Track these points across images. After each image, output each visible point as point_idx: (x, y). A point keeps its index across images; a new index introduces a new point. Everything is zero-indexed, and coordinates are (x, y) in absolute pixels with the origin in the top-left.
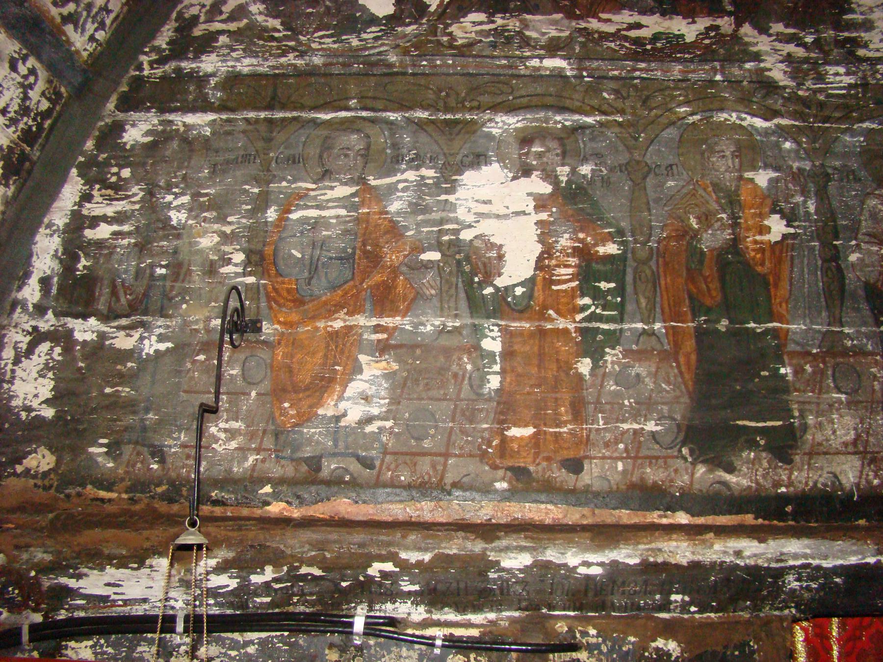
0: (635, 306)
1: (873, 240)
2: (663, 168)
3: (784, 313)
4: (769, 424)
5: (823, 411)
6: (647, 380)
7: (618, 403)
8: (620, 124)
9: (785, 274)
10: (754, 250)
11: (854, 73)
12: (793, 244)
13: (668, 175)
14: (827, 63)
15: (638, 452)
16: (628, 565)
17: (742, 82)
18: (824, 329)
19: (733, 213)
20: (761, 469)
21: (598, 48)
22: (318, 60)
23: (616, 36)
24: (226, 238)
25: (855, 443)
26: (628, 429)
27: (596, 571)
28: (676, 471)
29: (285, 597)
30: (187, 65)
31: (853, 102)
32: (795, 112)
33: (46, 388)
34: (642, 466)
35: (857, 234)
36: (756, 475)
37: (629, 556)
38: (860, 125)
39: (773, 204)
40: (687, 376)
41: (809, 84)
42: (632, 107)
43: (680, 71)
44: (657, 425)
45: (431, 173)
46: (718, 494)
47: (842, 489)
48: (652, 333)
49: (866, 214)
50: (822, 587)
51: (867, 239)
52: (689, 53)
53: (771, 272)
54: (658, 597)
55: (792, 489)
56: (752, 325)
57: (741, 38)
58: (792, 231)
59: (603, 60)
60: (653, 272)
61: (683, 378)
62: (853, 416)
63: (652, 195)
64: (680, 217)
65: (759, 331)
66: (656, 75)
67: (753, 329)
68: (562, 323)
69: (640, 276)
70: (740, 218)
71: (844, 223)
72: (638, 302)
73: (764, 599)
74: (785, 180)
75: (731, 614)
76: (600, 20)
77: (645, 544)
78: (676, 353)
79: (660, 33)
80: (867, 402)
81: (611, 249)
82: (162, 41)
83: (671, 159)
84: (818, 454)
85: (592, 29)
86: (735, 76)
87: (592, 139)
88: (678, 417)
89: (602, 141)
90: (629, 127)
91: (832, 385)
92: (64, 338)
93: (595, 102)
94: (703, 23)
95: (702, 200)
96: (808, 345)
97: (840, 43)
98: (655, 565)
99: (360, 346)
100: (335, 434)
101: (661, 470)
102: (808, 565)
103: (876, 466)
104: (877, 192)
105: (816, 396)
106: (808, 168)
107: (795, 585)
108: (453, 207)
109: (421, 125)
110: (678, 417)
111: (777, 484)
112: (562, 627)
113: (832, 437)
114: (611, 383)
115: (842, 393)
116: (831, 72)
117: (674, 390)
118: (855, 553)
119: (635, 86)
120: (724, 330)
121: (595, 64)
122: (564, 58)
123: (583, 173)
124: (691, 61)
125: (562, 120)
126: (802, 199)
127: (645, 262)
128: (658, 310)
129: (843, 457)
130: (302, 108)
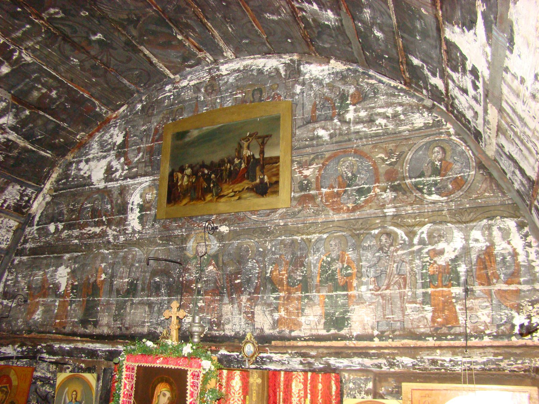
27: (68, 348)
45: (54, 268)
82: (22, 241)
97: (123, 230)
108: (56, 275)
112: (67, 360)
125: (75, 254)
130: (39, 255)
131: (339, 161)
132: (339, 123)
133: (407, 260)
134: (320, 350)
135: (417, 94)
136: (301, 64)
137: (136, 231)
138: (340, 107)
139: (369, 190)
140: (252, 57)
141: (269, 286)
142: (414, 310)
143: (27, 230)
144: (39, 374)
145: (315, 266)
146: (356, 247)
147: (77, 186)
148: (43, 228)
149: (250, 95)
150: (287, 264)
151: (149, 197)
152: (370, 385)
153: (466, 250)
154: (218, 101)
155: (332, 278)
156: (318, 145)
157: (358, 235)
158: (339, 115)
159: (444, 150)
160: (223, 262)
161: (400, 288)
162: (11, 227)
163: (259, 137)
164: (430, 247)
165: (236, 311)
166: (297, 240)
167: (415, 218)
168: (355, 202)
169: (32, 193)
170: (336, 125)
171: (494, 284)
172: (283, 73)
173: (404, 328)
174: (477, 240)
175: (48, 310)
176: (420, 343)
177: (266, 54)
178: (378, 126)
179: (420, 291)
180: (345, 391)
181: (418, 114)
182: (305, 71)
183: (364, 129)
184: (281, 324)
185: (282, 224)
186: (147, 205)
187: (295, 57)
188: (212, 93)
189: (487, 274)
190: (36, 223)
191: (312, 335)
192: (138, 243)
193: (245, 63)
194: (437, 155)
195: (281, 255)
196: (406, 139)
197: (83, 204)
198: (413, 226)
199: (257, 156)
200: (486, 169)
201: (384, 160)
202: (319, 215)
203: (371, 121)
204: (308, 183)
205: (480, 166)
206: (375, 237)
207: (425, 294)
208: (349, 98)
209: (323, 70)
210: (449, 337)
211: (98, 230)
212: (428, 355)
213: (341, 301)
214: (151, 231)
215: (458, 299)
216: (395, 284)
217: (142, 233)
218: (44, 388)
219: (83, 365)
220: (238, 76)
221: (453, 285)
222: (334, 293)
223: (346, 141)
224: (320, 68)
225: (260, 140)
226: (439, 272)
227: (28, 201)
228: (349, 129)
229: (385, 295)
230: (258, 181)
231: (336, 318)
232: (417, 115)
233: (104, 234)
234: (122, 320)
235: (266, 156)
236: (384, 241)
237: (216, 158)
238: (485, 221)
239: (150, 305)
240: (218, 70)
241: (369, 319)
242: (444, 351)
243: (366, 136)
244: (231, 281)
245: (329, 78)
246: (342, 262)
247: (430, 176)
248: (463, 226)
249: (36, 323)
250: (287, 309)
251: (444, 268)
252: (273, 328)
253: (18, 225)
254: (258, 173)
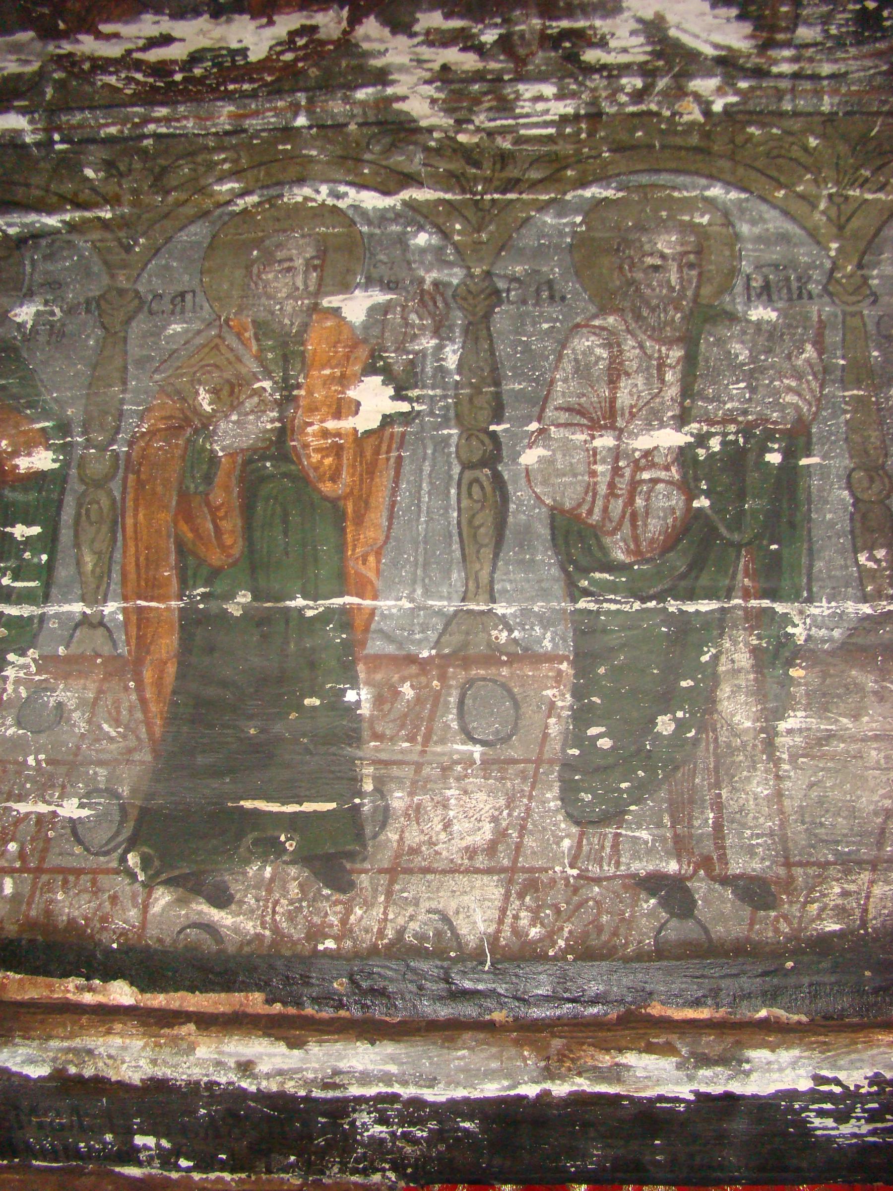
0: (72, 570)
1: (578, 419)
2: (167, 299)
3: (371, 575)
4: (308, 807)
5: (428, 780)
6: (76, 715)
7: (16, 762)
8: (105, 224)
9: (381, 499)
10: (317, 450)
11: (573, 95)
12: (403, 434)
13: (173, 313)
14: (520, 78)
15: (42, 859)
16: (27, 1077)
17: (346, 125)
18: (450, 607)
19: (285, 379)
20: (284, 902)
21: (88, 89)
23: (126, 62)
25: (491, 849)
26: (28, 814)
28: (114, 899)
31: (570, 149)
32: (451, 174)
34: (49, 888)
35: (543, 410)
36: (274, 912)
37: (31, 1061)
38: (580, 192)
39: (372, 356)
40: (153, 708)
41: (481, 119)
42: (135, 192)
43: (231, 116)
44: (81, 806)
46: (192, 948)
47: (460, 947)
48: (97, 623)
49: (568, 366)
50: (437, 1137)
51: (564, 417)
52: (252, 81)
53: (351, 493)
54: (109, 1137)
55: (349, 944)
56: (300, 602)
57: (357, 46)
58: (404, 407)
59: (92, 108)
60: (114, 502)
61: (145, 710)
62: (491, 792)
63: (134, 350)
64: (178, 392)
65: (310, 613)
66: (185, 127)
67: (300, 610)
69: (88, 510)
70: (298, 386)
71: (517, 387)
72: (79, 563)
73: (322, 1153)
74: (404, 307)
75: (264, 1176)
76: (99, 36)
77: (62, 1039)
78: (139, 662)
79: (204, 50)
80: (527, 761)
83: (185, 281)
84: (409, 871)
85: (83, 54)
86: (333, 117)
87: (48, 257)
88: (124, 791)
89: (65, 259)
90: (120, 228)
91: (455, 725)
93: (69, 187)
95: (230, 356)
96: (413, 642)
97: (551, 41)
98: (79, 1080)
101: (86, 896)
102: (394, 1098)
103: (537, 899)
104: (596, 323)
105: (419, 748)
106: (455, 281)
107: (378, 1130)
110: (124, 791)
111: (316, 933)
113: (443, 836)
114: (9, 721)
115: (475, 741)
116: (527, 95)
117: (124, 736)
118: (490, 1075)
119: (145, 151)
120: (237, 613)
121: (77, 118)
122: (23, 111)
123: (19, 320)
124: (254, 95)
126: (434, 342)
127: (99, 484)
128: (116, 576)
129: (463, 880)
137: (693, 56)
217: (759, 73)
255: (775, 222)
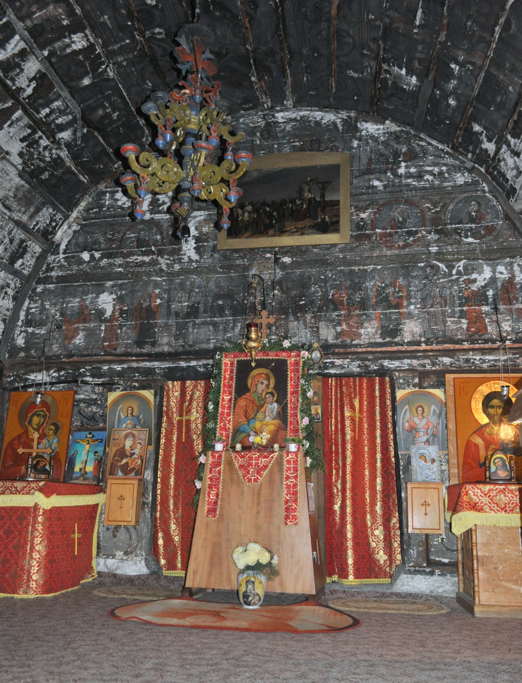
22: (74, 272)
23: (133, 262)
24: (56, 310)
27: (120, 369)
29: (66, 377)
30: (49, 274)
33: (23, 341)
45: (94, 295)
68: (116, 323)
81: (126, 308)
82: (44, 269)
92: (26, 331)
94: (150, 257)
97: (178, 259)
99: (80, 330)
100: (74, 346)
108: (97, 302)
109: (94, 285)
112: (116, 381)
125: (120, 282)
131: (392, 208)
132: (392, 176)
133: (447, 286)
134: (377, 355)
135: (460, 157)
136: (358, 121)
138: (393, 163)
139: (417, 232)
140: (309, 108)
141: (331, 306)
142: (453, 322)
143: (49, 258)
144: (82, 396)
145: (371, 290)
146: (406, 276)
147: (114, 216)
148: (73, 257)
149: (308, 144)
150: (346, 288)
151: (205, 229)
152: (417, 380)
153: (493, 280)
154: (276, 146)
155: (386, 299)
156: (373, 193)
157: (407, 267)
158: (392, 169)
159: (479, 204)
160: (287, 288)
161: (441, 307)
162: (35, 253)
163: (319, 183)
164: (465, 277)
165: (302, 327)
166: (355, 270)
167: (454, 255)
168: (405, 241)
169: (60, 219)
170: (389, 177)
171: (514, 304)
172: (341, 128)
173: (445, 336)
174: (501, 273)
175: (90, 334)
176: (457, 346)
177: (324, 107)
178: (425, 181)
179: (457, 309)
180: (396, 386)
181: (460, 174)
182: (362, 128)
183: (414, 183)
184: (343, 335)
185: (341, 257)
186: (204, 237)
187: (353, 114)
188: (268, 138)
189: (509, 297)
190: (61, 251)
191: (371, 343)
192: (195, 271)
193: (302, 113)
194: (473, 206)
195: (341, 282)
196: (448, 193)
197: (125, 234)
198: (452, 261)
199: (318, 199)
200: (512, 220)
201: (430, 209)
202: (374, 250)
203: (419, 176)
204: (364, 224)
205: (507, 217)
206: (422, 268)
207: (461, 311)
208: (402, 156)
209: (379, 129)
210: (480, 342)
211: (147, 259)
212: (463, 355)
213: (394, 317)
214: (210, 261)
215: (487, 314)
216: (437, 303)
218: (90, 409)
219: (137, 384)
220: (295, 125)
221: (483, 305)
222: (388, 311)
223: (398, 191)
224: (376, 127)
225: (321, 185)
226: (473, 295)
227: (54, 228)
228: (401, 181)
229: (430, 312)
230: (319, 220)
231: (391, 329)
232: (459, 175)
233: (154, 263)
234: (184, 339)
235: (326, 199)
236: (428, 271)
237: (278, 197)
238: (508, 259)
239: (215, 325)
240: (274, 116)
241: (418, 329)
242: (475, 352)
243: (415, 188)
244: (295, 302)
245: (384, 137)
246: (395, 287)
247: (467, 224)
248: (491, 262)
249: (77, 347)
250: (348, 324)
251: (476, 292)
252: (336, 338)
253: (41, 252)
254: (319, 213)
255: (200, 280)
